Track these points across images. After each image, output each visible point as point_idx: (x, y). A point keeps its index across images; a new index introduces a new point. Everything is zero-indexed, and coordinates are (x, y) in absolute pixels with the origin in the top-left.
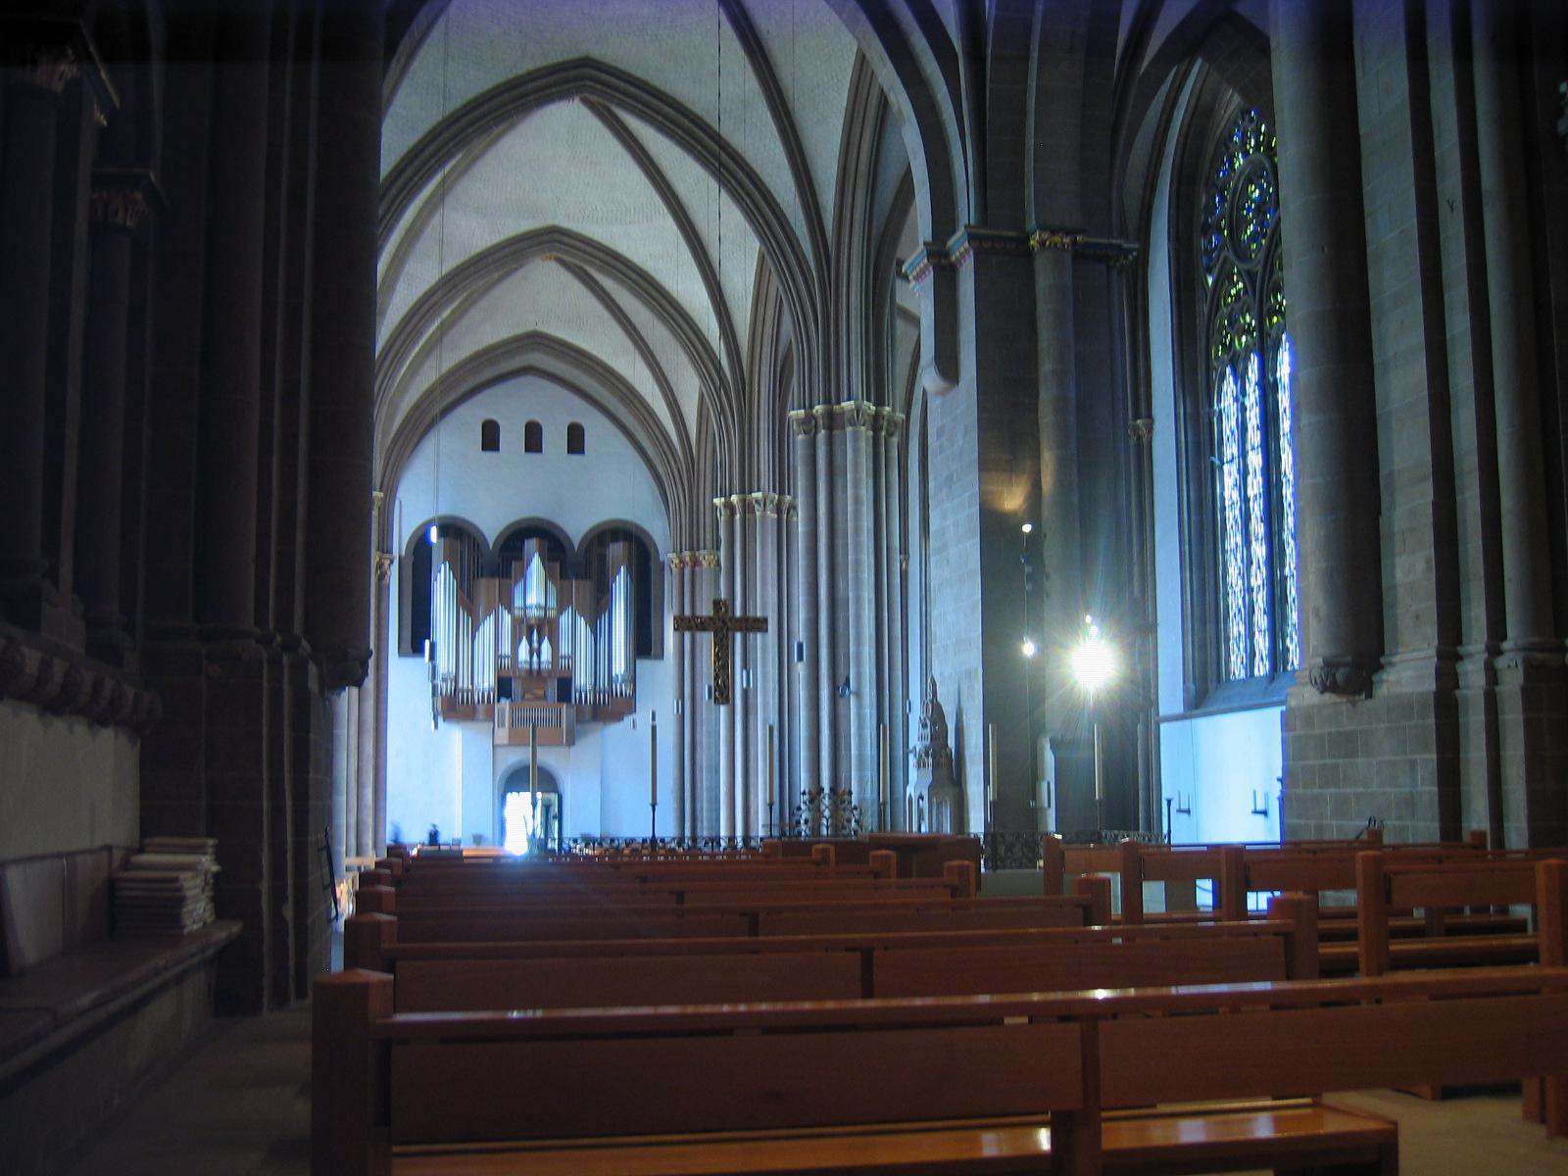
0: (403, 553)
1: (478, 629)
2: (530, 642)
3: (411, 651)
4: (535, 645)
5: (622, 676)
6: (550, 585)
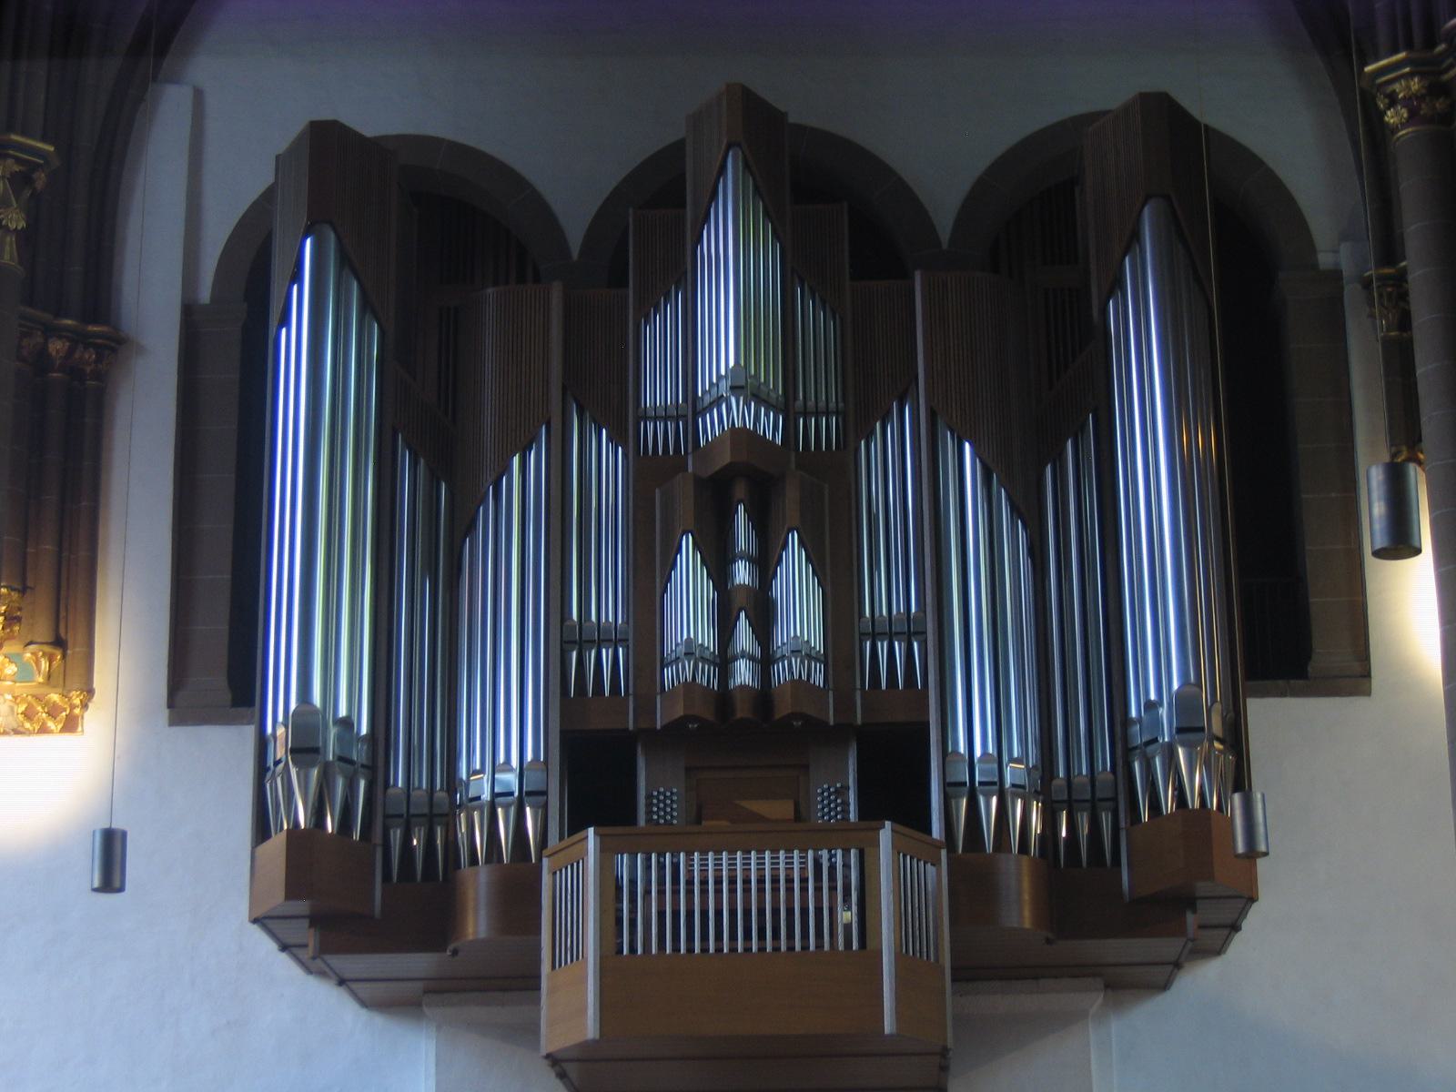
0: (205, 295)
1: (471, 528)
2: (718, 564)
3: (228, 697)
4: (742, 574)
5: (1186, 705)
6: (809, 311)
